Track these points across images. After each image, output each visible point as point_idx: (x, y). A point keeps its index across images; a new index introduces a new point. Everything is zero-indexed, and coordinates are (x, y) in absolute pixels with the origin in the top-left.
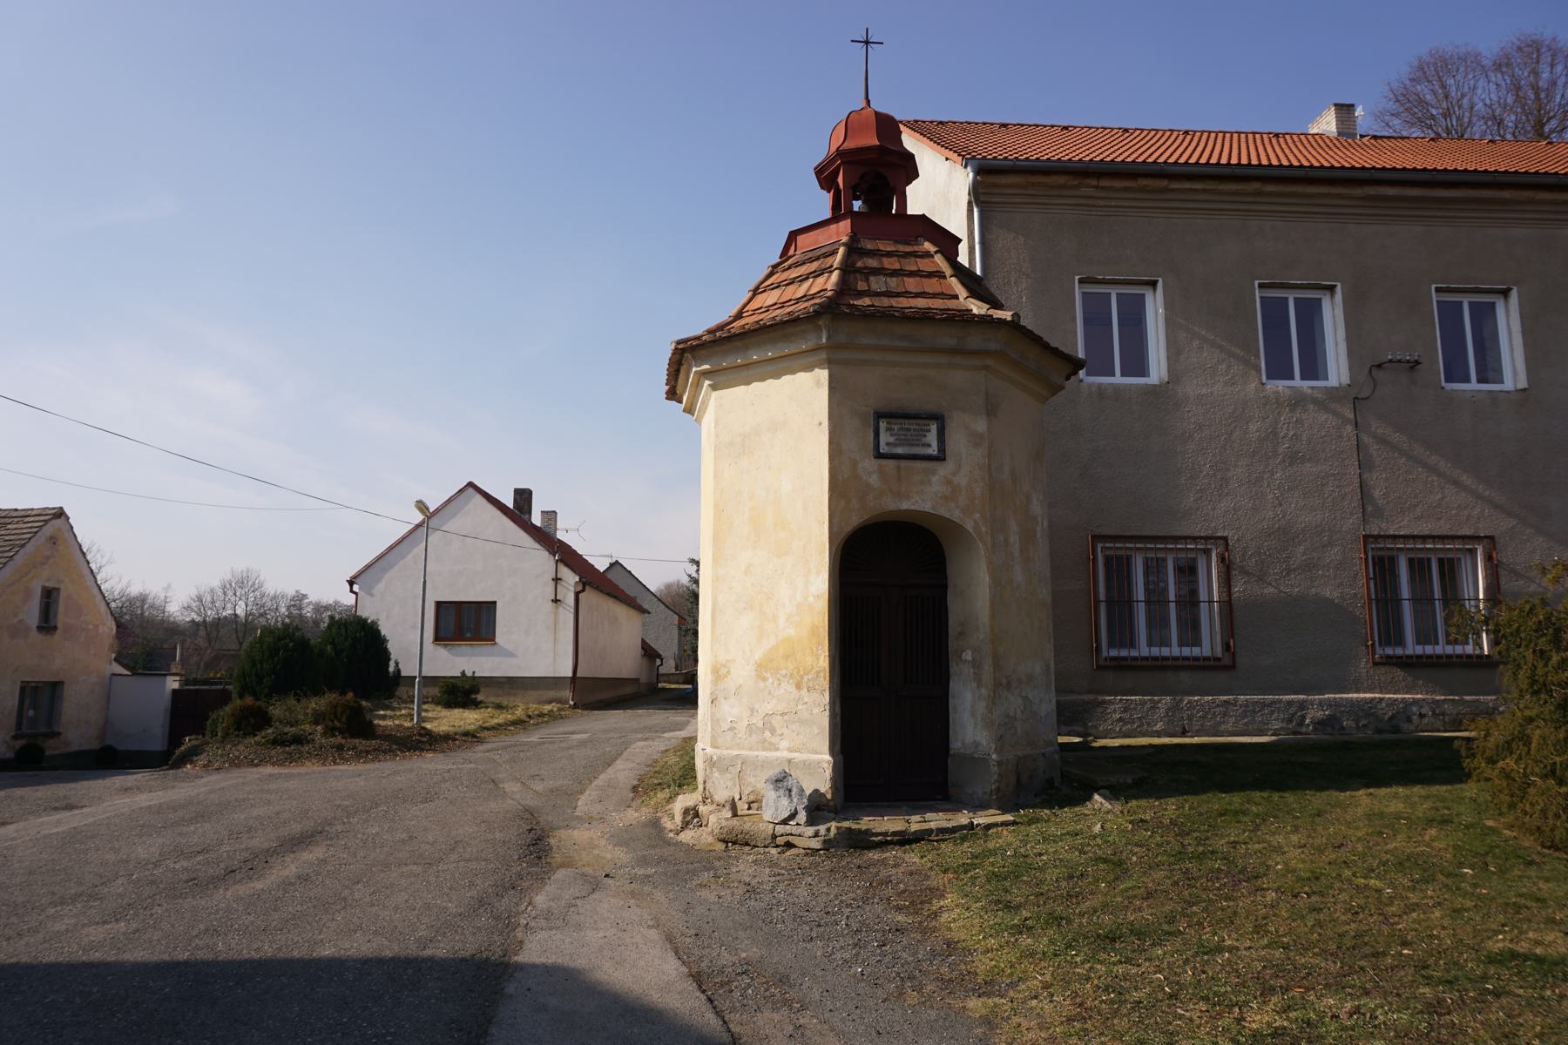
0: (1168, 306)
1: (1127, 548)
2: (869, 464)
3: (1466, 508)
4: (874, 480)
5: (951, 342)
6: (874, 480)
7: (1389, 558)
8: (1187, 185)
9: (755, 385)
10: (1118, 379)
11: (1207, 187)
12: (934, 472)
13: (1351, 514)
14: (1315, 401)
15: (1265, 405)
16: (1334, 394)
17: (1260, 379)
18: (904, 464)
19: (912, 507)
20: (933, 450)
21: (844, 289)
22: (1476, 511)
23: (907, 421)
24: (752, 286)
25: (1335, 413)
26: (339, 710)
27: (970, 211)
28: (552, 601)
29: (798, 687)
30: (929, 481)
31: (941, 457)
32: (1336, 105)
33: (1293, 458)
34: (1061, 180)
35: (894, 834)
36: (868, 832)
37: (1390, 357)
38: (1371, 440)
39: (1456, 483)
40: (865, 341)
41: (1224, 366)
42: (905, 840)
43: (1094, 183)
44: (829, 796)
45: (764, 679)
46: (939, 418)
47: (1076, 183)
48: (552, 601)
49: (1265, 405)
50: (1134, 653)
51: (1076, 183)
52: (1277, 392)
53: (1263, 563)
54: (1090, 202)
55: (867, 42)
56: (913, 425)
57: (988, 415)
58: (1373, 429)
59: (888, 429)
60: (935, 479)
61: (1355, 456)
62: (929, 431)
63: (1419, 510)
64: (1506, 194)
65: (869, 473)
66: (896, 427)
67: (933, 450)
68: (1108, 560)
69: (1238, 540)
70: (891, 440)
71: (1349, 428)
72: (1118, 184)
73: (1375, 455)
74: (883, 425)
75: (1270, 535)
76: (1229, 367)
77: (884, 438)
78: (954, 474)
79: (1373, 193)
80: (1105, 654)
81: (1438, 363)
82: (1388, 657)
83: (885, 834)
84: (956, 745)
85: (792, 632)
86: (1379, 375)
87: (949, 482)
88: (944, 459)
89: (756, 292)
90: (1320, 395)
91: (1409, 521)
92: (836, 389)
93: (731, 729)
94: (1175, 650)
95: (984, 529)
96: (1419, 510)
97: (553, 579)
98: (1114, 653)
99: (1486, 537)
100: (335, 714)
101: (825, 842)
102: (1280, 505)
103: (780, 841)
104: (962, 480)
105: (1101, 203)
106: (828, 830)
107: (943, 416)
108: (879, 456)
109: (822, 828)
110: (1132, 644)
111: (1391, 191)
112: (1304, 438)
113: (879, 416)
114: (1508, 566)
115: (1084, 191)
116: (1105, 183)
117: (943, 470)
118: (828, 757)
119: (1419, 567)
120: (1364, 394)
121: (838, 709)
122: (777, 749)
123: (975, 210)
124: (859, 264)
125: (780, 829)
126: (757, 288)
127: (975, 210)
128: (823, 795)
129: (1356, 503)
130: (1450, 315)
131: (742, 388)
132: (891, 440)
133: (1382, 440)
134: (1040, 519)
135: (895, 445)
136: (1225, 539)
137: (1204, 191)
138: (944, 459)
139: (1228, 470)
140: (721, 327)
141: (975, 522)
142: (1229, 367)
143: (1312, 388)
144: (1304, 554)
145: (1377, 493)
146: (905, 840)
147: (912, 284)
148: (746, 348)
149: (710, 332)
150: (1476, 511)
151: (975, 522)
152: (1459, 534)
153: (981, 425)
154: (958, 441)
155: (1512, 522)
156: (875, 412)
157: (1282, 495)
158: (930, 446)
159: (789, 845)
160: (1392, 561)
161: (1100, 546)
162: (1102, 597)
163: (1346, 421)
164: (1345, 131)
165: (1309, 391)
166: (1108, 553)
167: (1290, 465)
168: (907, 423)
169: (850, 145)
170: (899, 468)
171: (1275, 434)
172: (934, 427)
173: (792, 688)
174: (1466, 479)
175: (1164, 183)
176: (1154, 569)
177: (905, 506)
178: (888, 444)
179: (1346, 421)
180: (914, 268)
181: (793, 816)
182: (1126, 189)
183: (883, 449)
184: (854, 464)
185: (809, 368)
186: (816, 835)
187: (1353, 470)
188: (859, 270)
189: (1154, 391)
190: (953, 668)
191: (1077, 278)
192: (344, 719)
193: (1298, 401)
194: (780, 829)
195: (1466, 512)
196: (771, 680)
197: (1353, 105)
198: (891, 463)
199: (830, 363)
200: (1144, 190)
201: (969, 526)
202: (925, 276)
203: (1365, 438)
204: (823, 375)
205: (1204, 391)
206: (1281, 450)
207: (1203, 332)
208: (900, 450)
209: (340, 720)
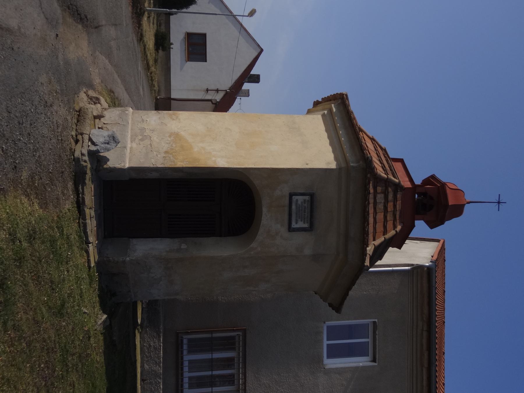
0: (364, 368)
2: (285, 190)
8: (425, 378)
10: (326, 342)
18: (287, 209)
19: (264, 213)
20: (294, 225)
21: (378, 179)
28: (207, 89)
29: (166, 152)
31: (290, 229)
35: (83, 199)
36: (84, 184)
42: (80, 205)
43: (425, 329)
44: (105, 166)
45: (170, 136)
46: (311, 228)
48: (207, 89)
50: (185, 352)
55: (499, 203)
59: (305, 200)
62: (304, 223)
67: (294, 225)
68: (233, 338)
70: (299, 202)
72: (425, 341)
74: (307, 198)
77: (300, 199)
80: (185, 337)
83: (83, 193)
84: (134, 241)
85: (196, 150)
89: (372, 140)
93: (143, 121)
94: (187, 375)
95: (252, 253)
97: (218, 89)
98: (185, 341)
101: (78, 159)
103: (80, 137)
106: (85, 161)
108: (291, 195)
109: (86, 158)
110: (190, 352)
113: (312, 196)
116: (425, 334)
117: (283, 230)
118: (127, 166)
122: (132, 142)
123: (409, 268)
124: (390, 189)
125: (86, 137)
127: (409, 268)
128: (106, 163)
132: (299, 202)
134: (256, 289)
135: (297, 204)
138: (289, 231)
146: (80, 205)
147: (380, 216)
153: (307, 251)
154: (299, 238)
156: (314, 193)
158: (296, 223)
159: (77, 142)
161: (240, 333)
162: (215, 335)
172: (306, 225)
173: (165, 149)
175: (426, 365)
176: (228, 363)
177: (265, 210)
178: (297, 200)
180: (388, 218)
181: (93, 143)
183: (295, 198)
185: (336, 159)
186: (83, 155)
188: (387, 189)
189: (320, 361)
190: (176, 240)
191: (376, 320)
194: (86, 137)
196: (169, 139)
198: (287, 202)
199: (339, 169)
201: (254, 245)
204: (333, 165)
208: (294, 207)
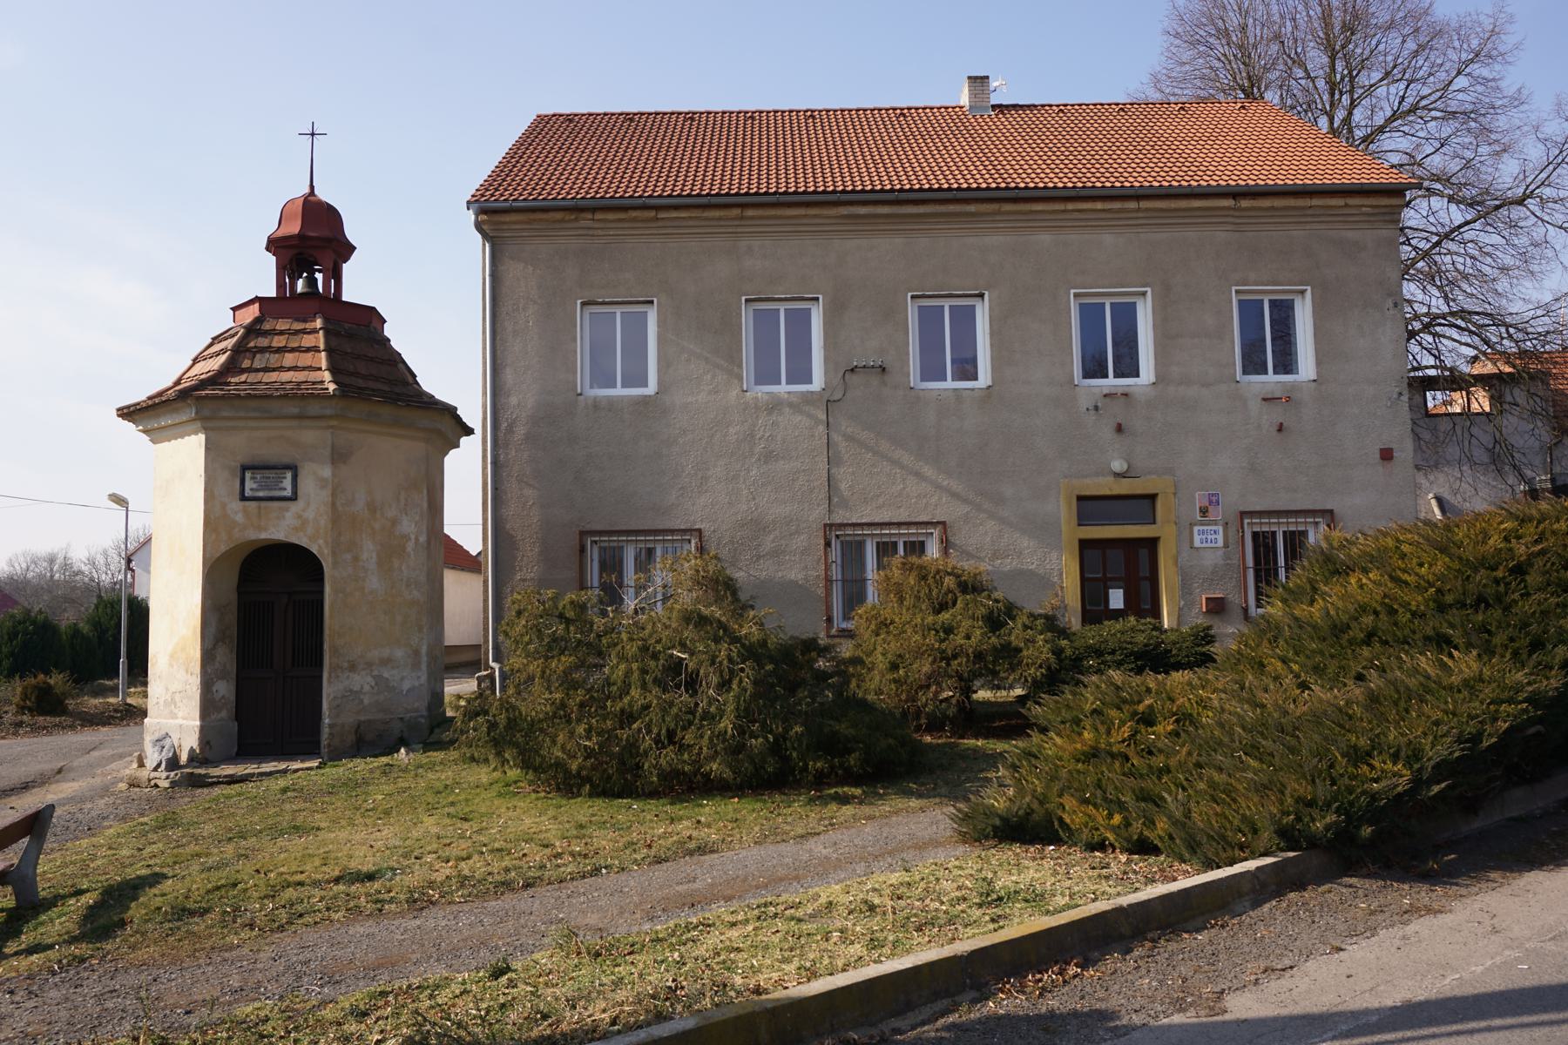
0: (661, 323)
1: (619, 541)
2: (236, 505)
3: (925, 496)
4: (239, 518)
5: (296, 411)
6: (239, 518)
7: (1083, 520)
8: (674, 214)
9: (187, 438)
10: (619, 391)
11: (693, 215)
12: (287, 510)
13: (818, 505)
14: (791, 405)
15: (744, 410)
16: (808, 398)
17: (742, 387)
18: (263, 504)
19: (269, 537)
20: (288, 493)
21: (230, 368)
22: (933, 500)
23: (267, 471)
24: (193, 356)
25: (809, 416)
26: (29, 691)
27: (484, 245)
30: (284, 517)
31: (294, 498)
32: (969, 78)
33: (768, 457)
34: (559, 215)
35: (226, 776)
36: (207, 776)
37: (855, 364)
38: (840, 438)
39: (917, 474)
40: (225, 414)
41: (709, 377)
42: (232, 780)
43: (590, 216)
44: (198, 751)
46: (294, 469)
47: (573, 217)
49: (744, 410)
51: (573, 217)
52: (757, 398)
53: (735, 550)
54: (591, 232)
55: (313, 134)
56: (271, 474)
57: (333, 464)
58: (843, 428)
59: (252, 478)
60: (288, 515)
61: (825, 453)
62: (285, 478)
63: (881, 500)
64: (972, 208)
65: (236, 513)
66: (258, 476)
67: (288, 493)
69: (714, 531)
70: (255, 486)
71: (822, 428)
72: (611, 216)
73: (843, 452)
74: (248, 475)
75: (743, 526)
76: (714, 377)
77: (249, 484)
78: (303, 511)
79: (846, 213)
81: (909, 366)
82: (844, 630)
83: (219, 777)
86: (853, 379)
87: (300, 517)
88: (296, 499)
89: (195, 361)
90: (795, 399)
91: (872, 510)
92: (209, 448)
93: (157, 703)
95: (326, 551)
96: (881, 500)
99: (938, 523)
100: (26, 695)
101: (171, 782)
102: (754, 499)
103: (152, 783)
104: (310, 514)
105: (600, 232)
106: (176, 775)
107: (296, 467)
108: (243, 498)
109: (172, 774)
111: (863, 210)
112: (779, 438)
113: (244, 468)
114: (960, 547)
115: (583, 223)
116: (599, 216)
117: (294, 507)
119: (886, 549)
120: (837, 396)
121: (225, 689)
122: (177, 718)
123: (487, 245)
124: (252, 344)
125: (153, 775)
126: (196, 358)
127: (487, 245)
128: (195, 750)
129: (823, 494)
130: (930, 319)
131: (167, 443)
133: (850, 438)
134: (413, 537)
135: (257, 490)
136: (700, 531)
137: (690, 218)
139: (708, 469)
140: (160, 394)
141: (320, 546)
142: (714, 377)
143: (789, 393)
144: (773, 541)
145: (843, 486)
146: (232, 780)
147: (289, 359)
148: (158, 416)
149: (150, 398)
150: (933, 500)
151: (320, 546)
152: (917, 520)
153: (326, 472)
154: (307, 485)
155: (965, 509)
156: (242, 466)
157: (756, 490)
158: (285, 489)
159: (156, 786)
160: (860, 545)
163: (818, 422)
164: (978, 104)
165: (786, 396)
167: (765, 463)
168: (267, 473)
169: (280, 234)
170: (259, 508)
171: (752, 436)
172: (289, 475)
174: (928, 471)
175: (652, 214)
177: (263, 536)
178: (252, 489)
179: (818, 422)
180: (296, 345)
181: (159, 765)
182: (620, 220)
183: (248, 493)
184: (224, 506)
185: (196, 433)
186: (167, 778)
187: (822, 465)
188: (249, 350)
189: (645, 400)
191: (579, 302)
192: (33, 699)
193: (775, 405)
194: (153, 775)
195: (924, 501)
197: (987, 77)
199: (206, 430)
200: (635, 220)
202: (303, 351)
203: (835, 437)
204: (201, 437)
205: (690, 400)
206: (757, 450)
207: (691, 347)
208: (261, 494)
209: (30, 700)
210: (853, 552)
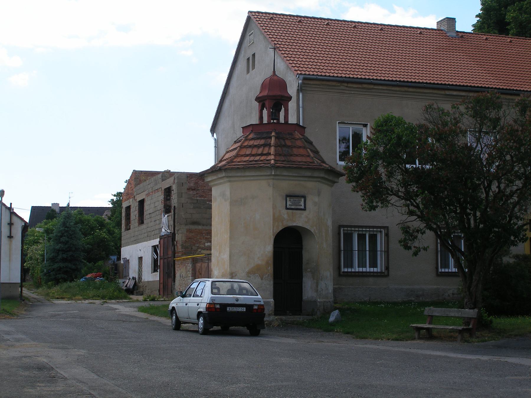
2: (285, 211)
4: (286, 216)
6: (286, 216)
8: (381, 87)
18: (294, 211)
20: (303, 207)
23: (295, 198)
28: (8, 237)
29: (262, 279)
31: (305, 209)
34: (334, 84)
40: (285, 174)
43: (346, 85)
45: (250, 277)
46: (304, 197)
48: (8, 237)
50: (353, 270)
54: (344, 91)
60: (303, 216)
66: (292, 200)
67: (303, 207)
68: (344, 234)
70: (291, 204)
74: (288, 199)
77: (289, 203)
80: (343, 270)
84: (305, 298)
85: (260, 262)
94: (368, 269)
95: (316, 232)
97: (13, 224)
98: (346, 270)
108: (287, 209)
110: (352, 267)
111: (455, 93)
113: (287, 196)
115: (342, 87)
116: (350, 85)
117: (305, 213)
118: (272, 300)
132: (291, 204)
135: (292, 205)
137: (387, 89)
138: (306, 210)
141: (315, 230)
151: (315, 230)
153: (316, 199)
154: (309, 204)
161: (342, 229)
162: (342, 249)
166: (346, 232)
170: (293, 213)
172: (303, 200)
173: (259, 280)
176: (362, 237)
177: (294, 224)
190: (304, 274)
191: (338, 122)
196: (252, 277)
198: (290, 211)
201: (312, 231)
208: (293, 207)
210: (348, 237)
